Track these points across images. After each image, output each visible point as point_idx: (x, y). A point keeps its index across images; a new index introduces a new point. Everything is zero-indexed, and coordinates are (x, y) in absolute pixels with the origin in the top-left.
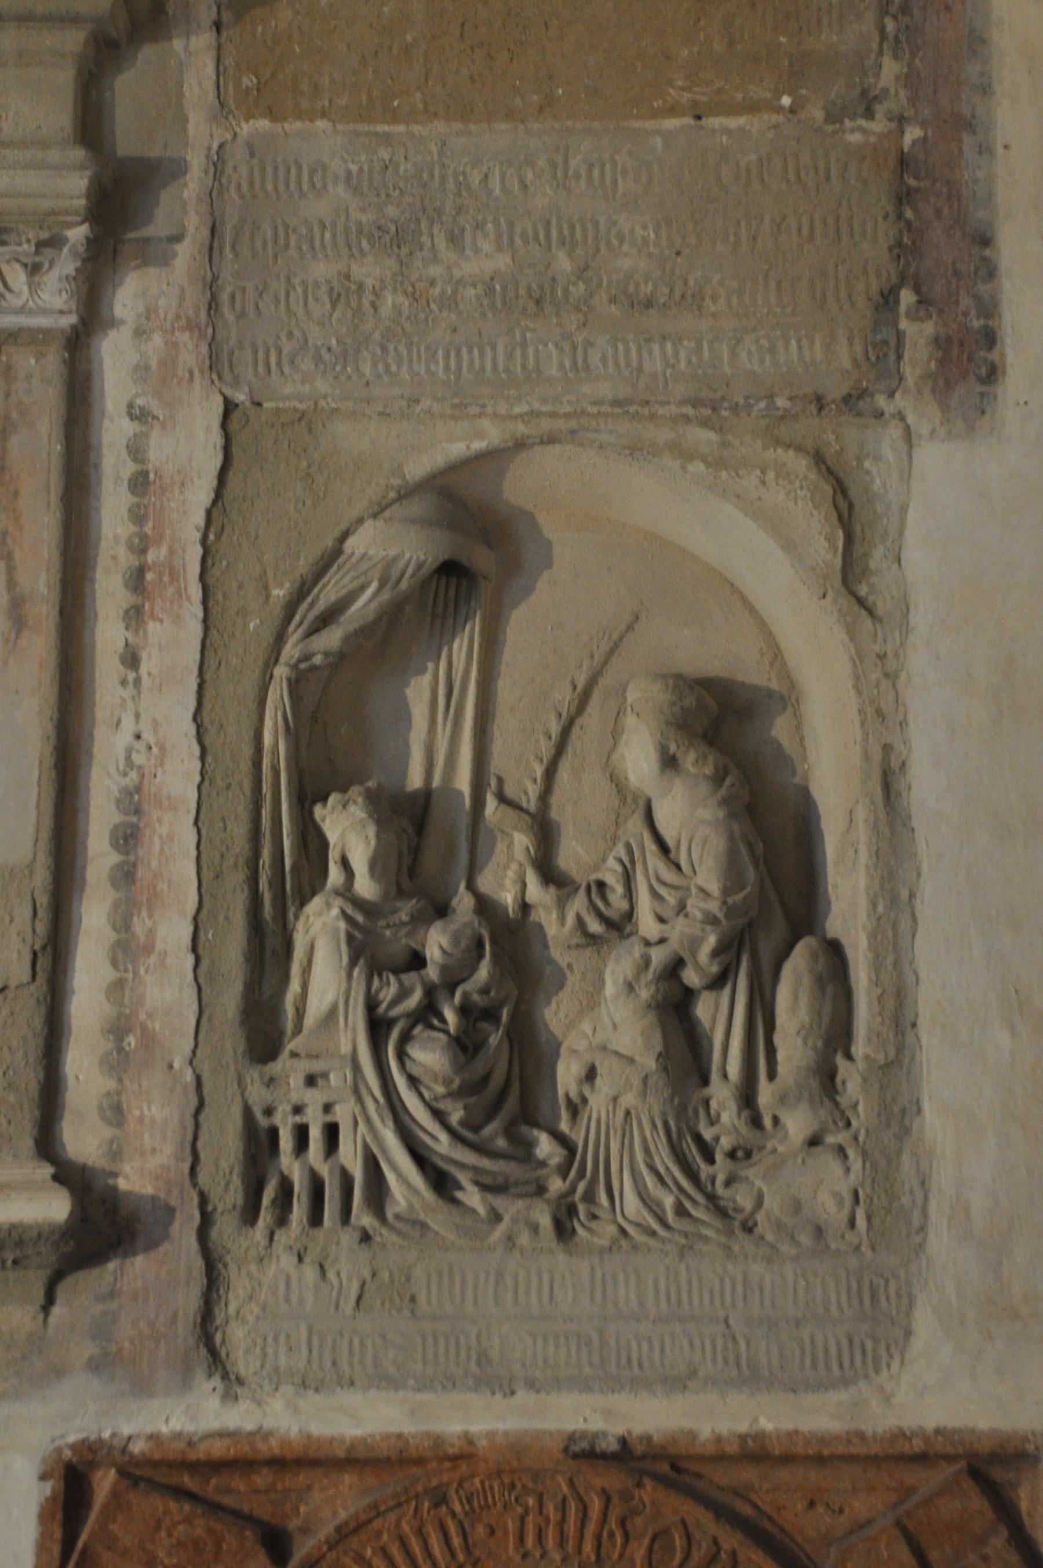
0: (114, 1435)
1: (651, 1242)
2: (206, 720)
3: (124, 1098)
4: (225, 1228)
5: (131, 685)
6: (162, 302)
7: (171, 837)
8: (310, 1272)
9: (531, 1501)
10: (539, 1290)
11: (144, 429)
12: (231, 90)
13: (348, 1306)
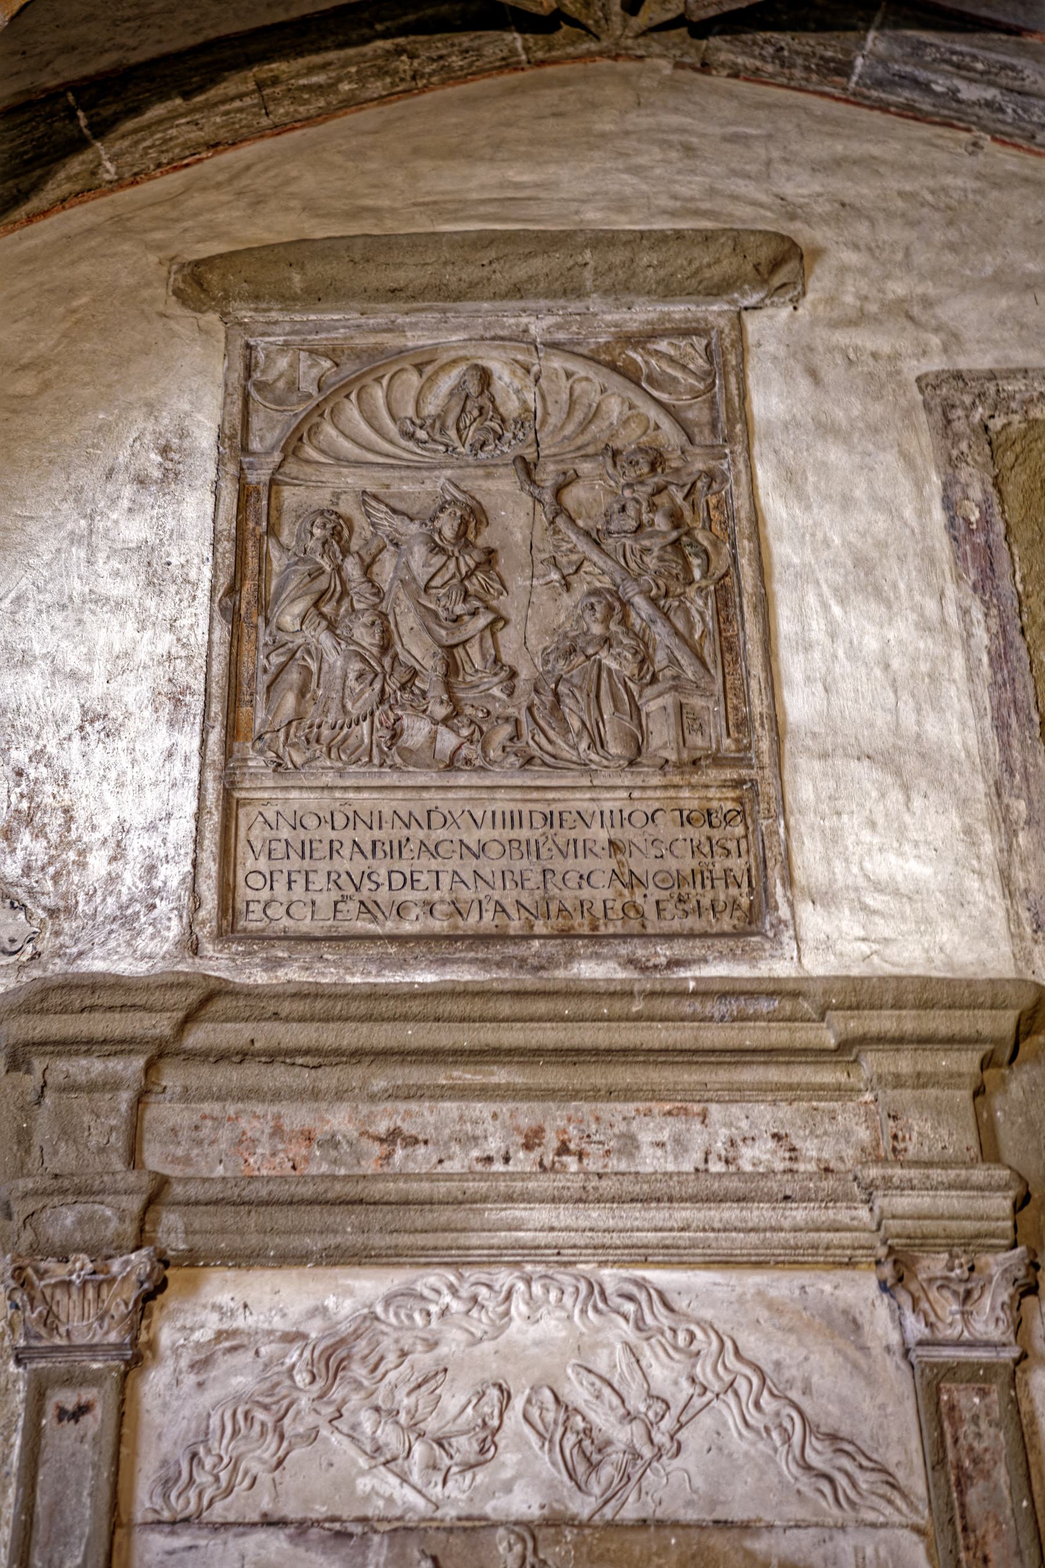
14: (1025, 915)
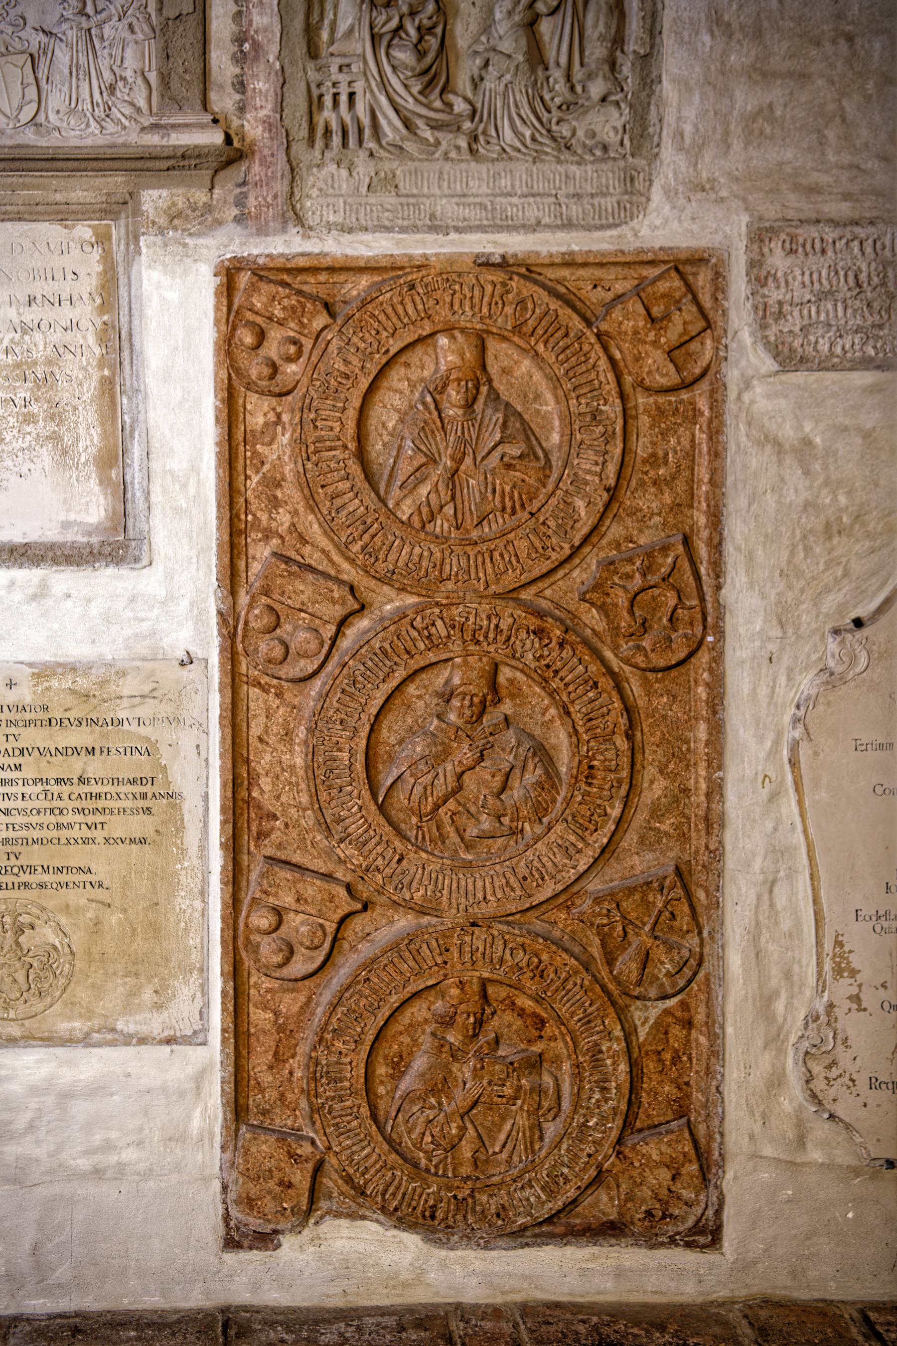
1: (519, 155)
4: (299, 149)
8: (344, 173)
9: (457, 287)
10: (461, 181)
13: (364, 190)
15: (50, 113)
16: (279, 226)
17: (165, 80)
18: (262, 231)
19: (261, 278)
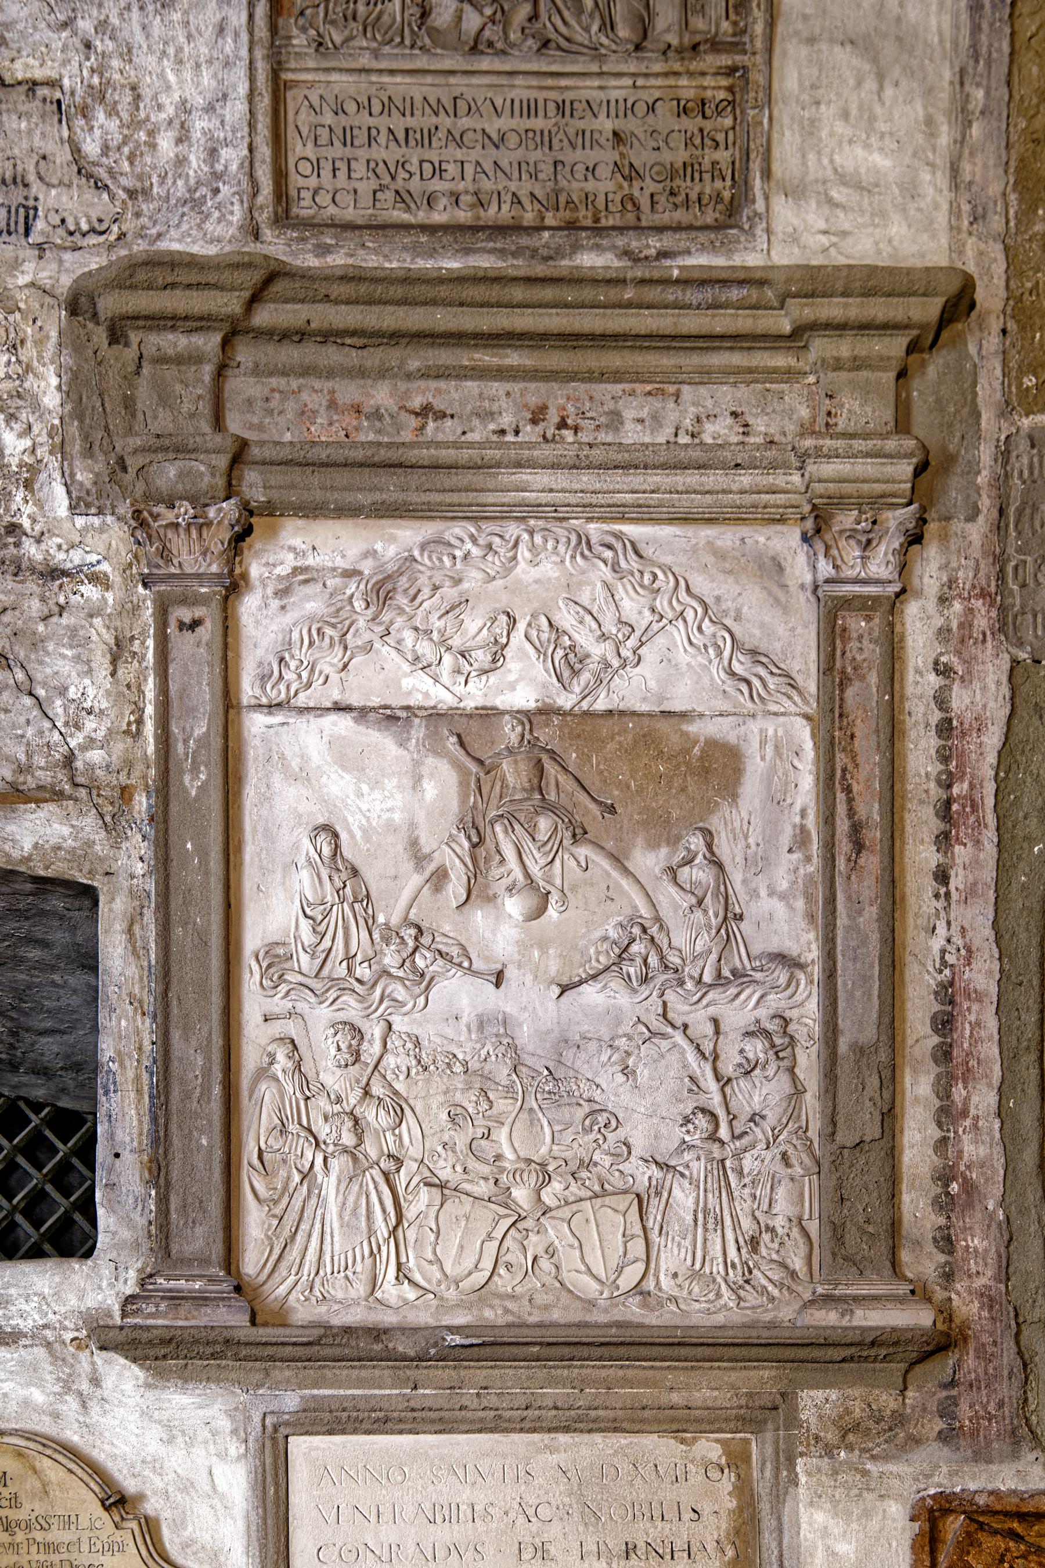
0: (963, 1490)
2: (1002, 927)
3: (952, 1231)
5: (943, 898)
6: (960, 574)
7: (978, 1024)
11: (947, 682)
12: (1014, 389)
14: (966, 208)
15: (662, 1277)
16: (1007, 1448)
17: (836, 1231)
18: (981, 1456)
19: (981, 1526)
